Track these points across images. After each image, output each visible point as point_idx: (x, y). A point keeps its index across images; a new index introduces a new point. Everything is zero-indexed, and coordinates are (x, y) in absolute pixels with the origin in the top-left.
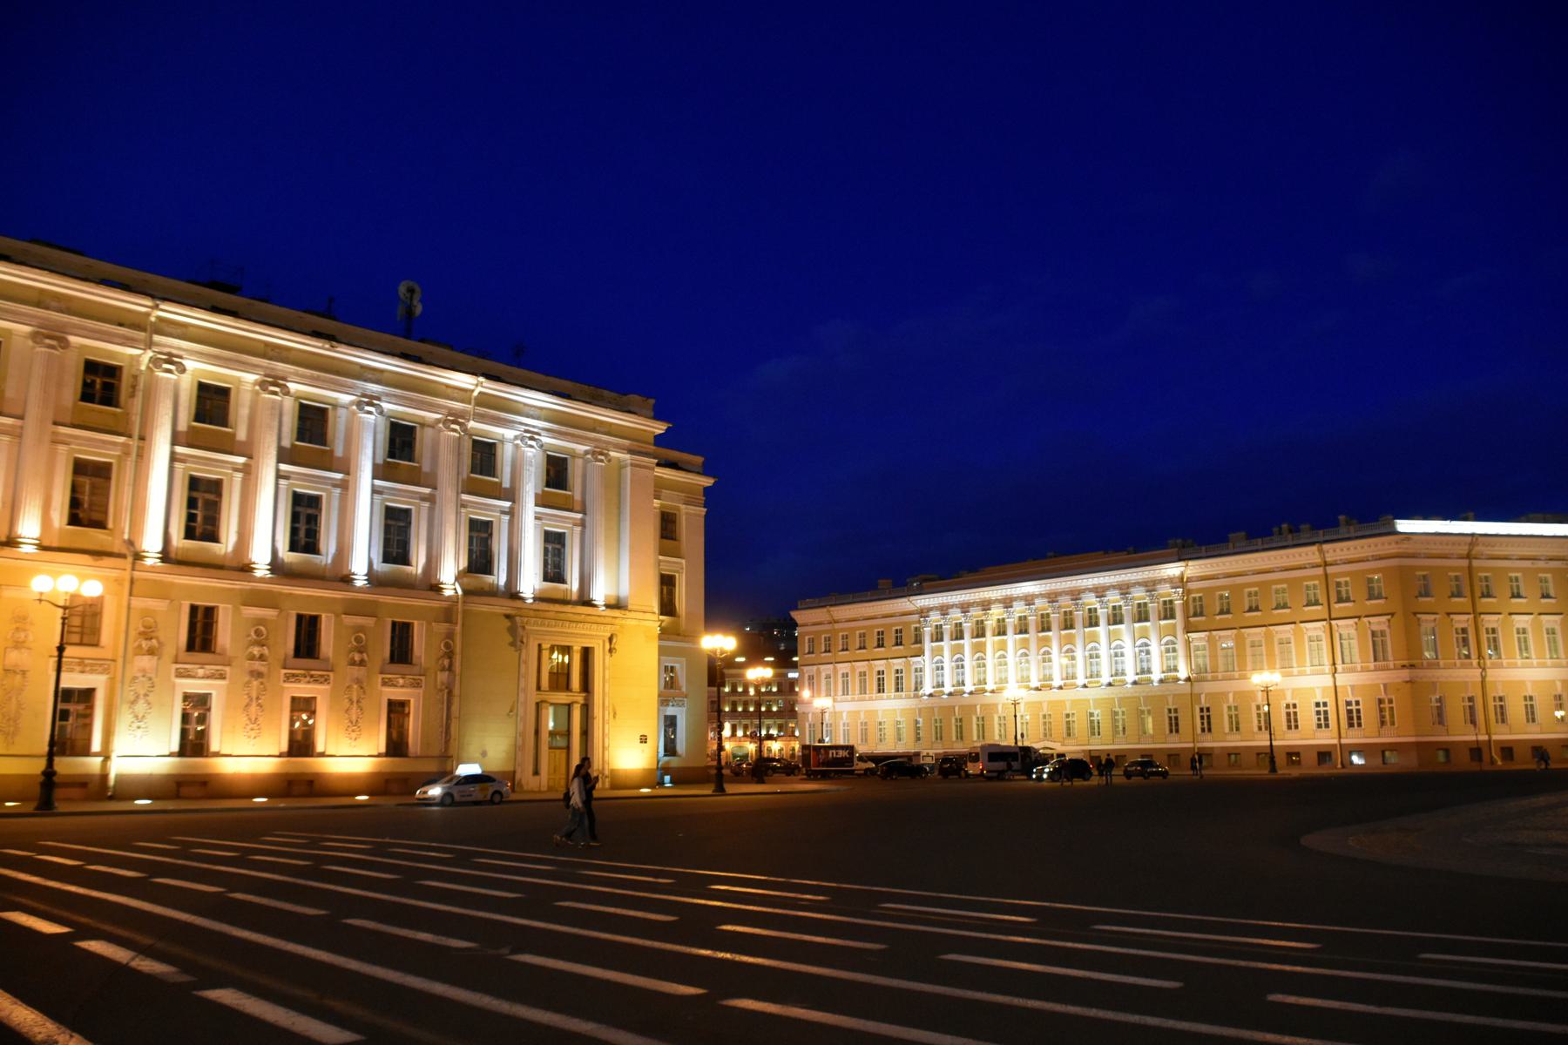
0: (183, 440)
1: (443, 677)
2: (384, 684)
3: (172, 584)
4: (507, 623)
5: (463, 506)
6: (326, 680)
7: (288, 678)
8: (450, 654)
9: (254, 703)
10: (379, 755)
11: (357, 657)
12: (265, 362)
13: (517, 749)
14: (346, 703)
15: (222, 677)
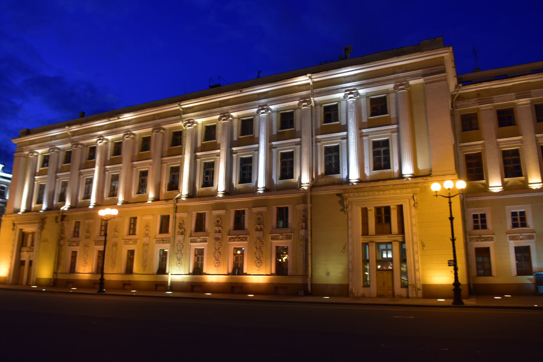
0: (199, 150)
1: (302, 232)
2: (273, 238)
3: (189, 206)
4: (339, 199)
5: (319, 142)
6: (246, 239)
7: (230, 240)
8: (305, 221)
9: (217, 252)
10: (272, 275)
11: (259, 227)
12: (219, 109)
13: (350, 271)
14: (255, 250)
15: (206, 241)
